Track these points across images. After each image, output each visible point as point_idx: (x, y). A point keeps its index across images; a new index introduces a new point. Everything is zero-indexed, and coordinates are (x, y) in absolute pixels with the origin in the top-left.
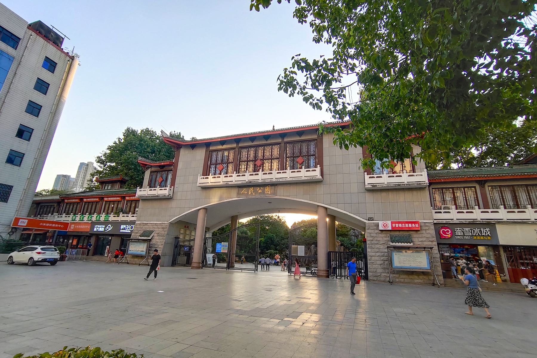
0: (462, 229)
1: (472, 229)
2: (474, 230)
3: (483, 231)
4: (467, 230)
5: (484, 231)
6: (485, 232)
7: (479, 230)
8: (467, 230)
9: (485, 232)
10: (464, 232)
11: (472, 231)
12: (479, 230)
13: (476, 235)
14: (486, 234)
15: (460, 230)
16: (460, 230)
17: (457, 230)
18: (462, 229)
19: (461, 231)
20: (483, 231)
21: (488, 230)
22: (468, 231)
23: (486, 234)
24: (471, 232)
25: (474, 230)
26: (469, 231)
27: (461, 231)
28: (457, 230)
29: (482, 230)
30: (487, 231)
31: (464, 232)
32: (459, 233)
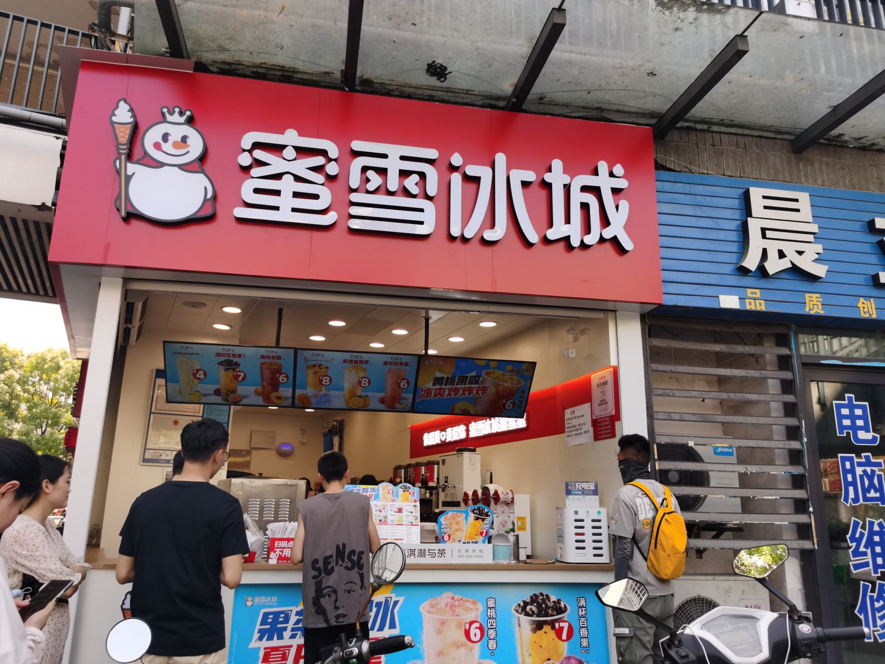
0: (333, 151)
1: (456, 159)
2: (472, 170)
3: (567, 188)
4: (394, 165)
5: (578, 198)
6: (585, 207)
7: (530, 176)
8: (394, 165)
9: (585, 207)
10: (355, 182)
11: (456, 178)
12: (530, 176)
13: (489, 235)
14: (587, 229)
15: (302, 152)
16: (302, 152)
17: (277, 149)
18: (333, 151)
19: (318, 169)
20: (567, 188)
21: (604, 182)
22: (404, 174)
23: (587, 229)
24: (432, 190)
25: (476, 180)
26: (411, 183)
27: (318, 169)
28: (277, 149)
29: (557, 177)
30: (596, 191)
31: (355, 182)
32: (287, 194)
